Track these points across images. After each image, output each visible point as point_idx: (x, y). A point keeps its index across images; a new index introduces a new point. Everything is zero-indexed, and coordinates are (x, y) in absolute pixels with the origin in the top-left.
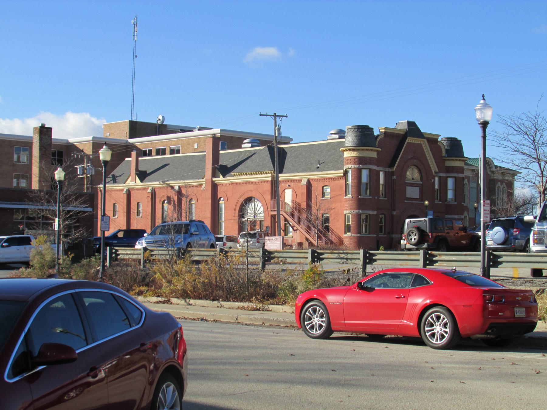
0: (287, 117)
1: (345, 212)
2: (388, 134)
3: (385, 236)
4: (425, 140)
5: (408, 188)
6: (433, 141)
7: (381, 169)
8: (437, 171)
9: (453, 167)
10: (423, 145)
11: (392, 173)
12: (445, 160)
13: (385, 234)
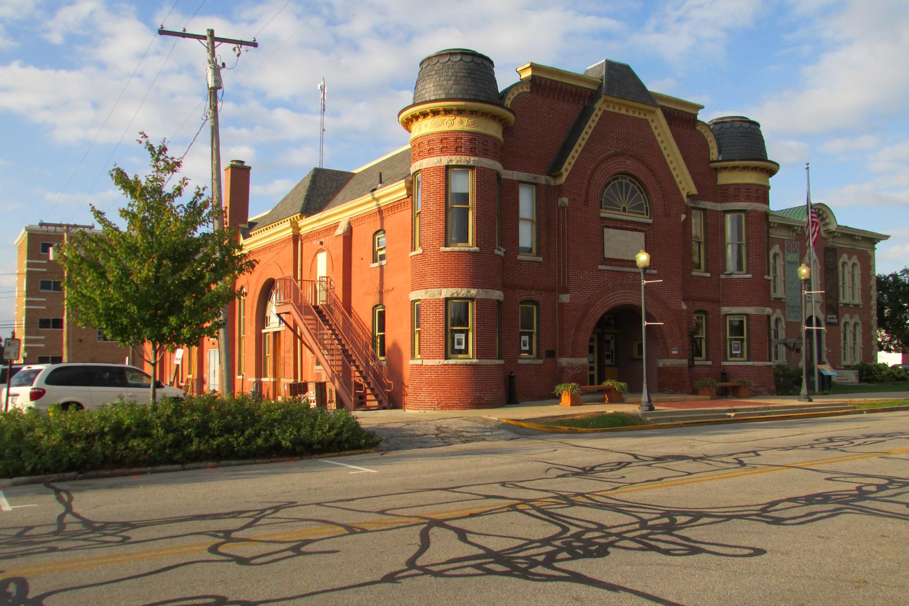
0: (255, 45)
1: (414, 296)
2: (544, 84)
3: (540, 361)
4: (659, 112)
5: (609, 233)
6: (682, 118)
7: (523, 176)
8: (694, 191)
9: (737, 187)
10: (653, 125)
11: (559, 190)
12: (716, 170)
13: (538, 357)
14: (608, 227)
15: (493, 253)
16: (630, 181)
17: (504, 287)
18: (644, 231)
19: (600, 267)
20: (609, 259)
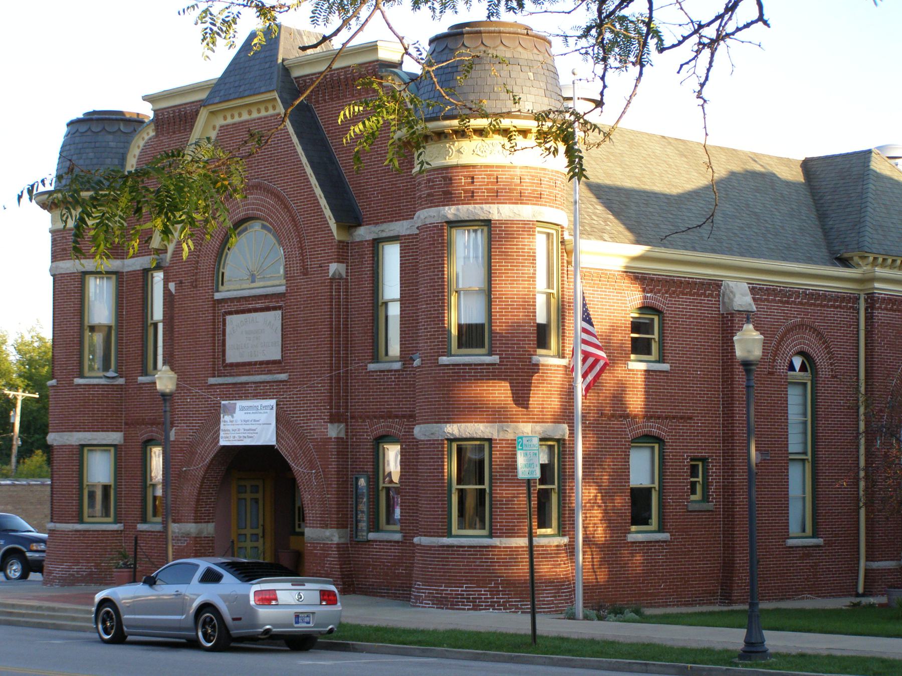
14: (231, 313)
15: (71, 384)
16: (264, 227)
17: (128, 425)
18: (280, 308)
19: (212, 381)
20: (238, 365)
